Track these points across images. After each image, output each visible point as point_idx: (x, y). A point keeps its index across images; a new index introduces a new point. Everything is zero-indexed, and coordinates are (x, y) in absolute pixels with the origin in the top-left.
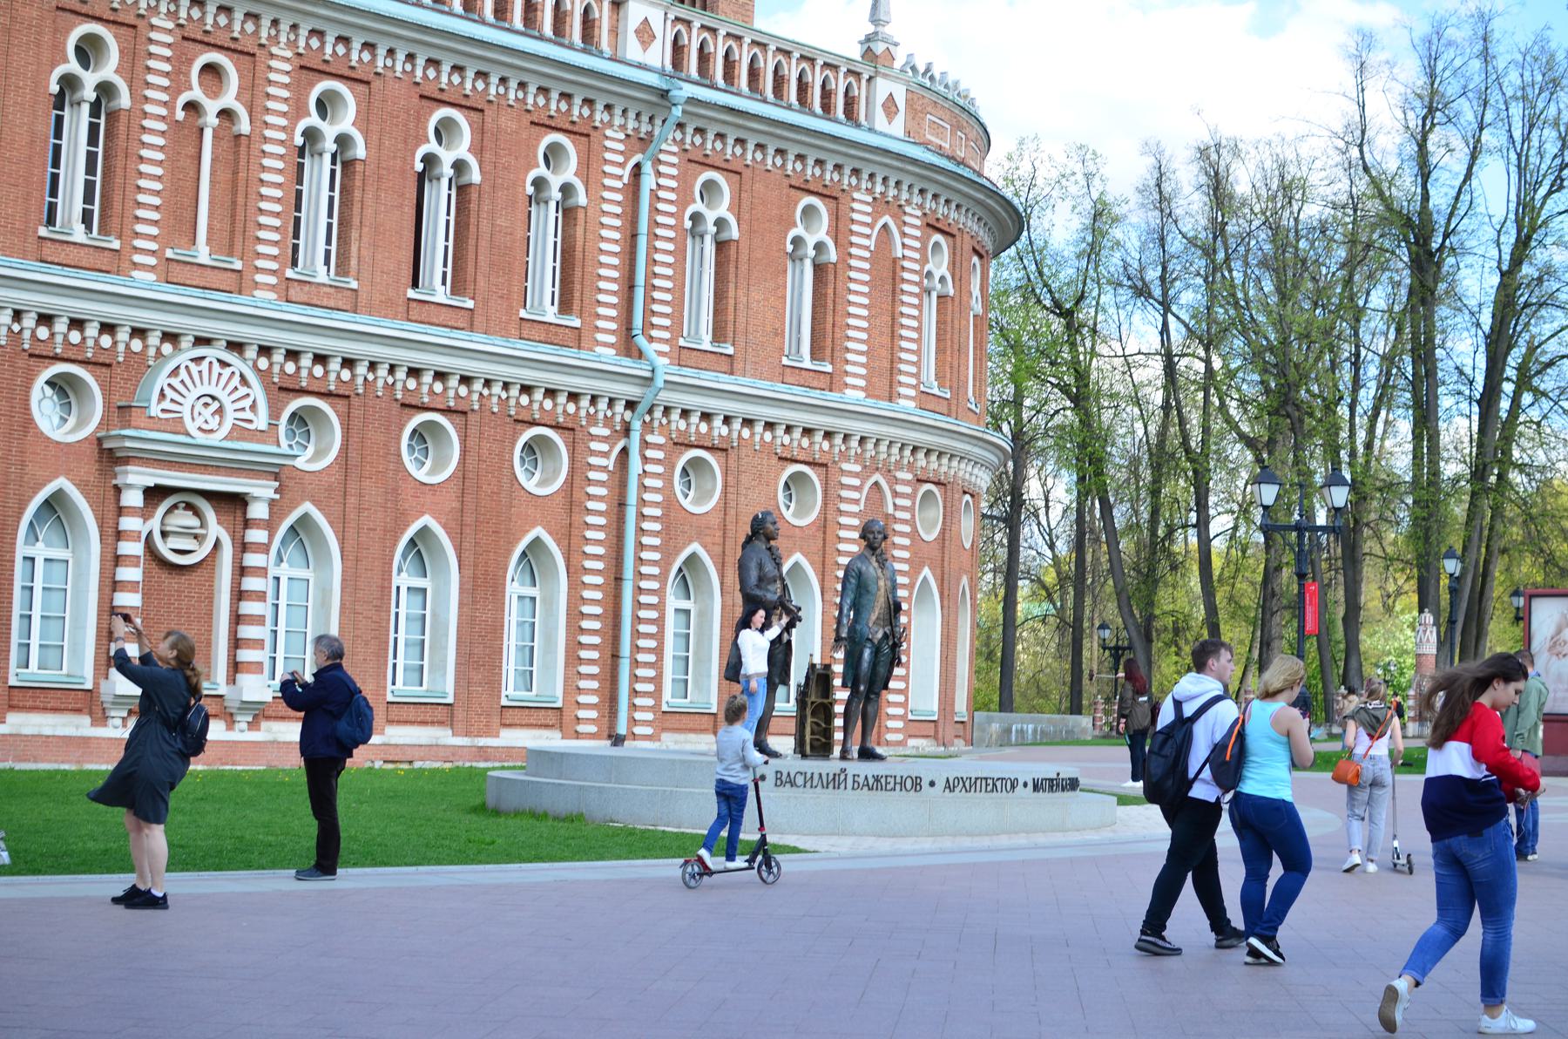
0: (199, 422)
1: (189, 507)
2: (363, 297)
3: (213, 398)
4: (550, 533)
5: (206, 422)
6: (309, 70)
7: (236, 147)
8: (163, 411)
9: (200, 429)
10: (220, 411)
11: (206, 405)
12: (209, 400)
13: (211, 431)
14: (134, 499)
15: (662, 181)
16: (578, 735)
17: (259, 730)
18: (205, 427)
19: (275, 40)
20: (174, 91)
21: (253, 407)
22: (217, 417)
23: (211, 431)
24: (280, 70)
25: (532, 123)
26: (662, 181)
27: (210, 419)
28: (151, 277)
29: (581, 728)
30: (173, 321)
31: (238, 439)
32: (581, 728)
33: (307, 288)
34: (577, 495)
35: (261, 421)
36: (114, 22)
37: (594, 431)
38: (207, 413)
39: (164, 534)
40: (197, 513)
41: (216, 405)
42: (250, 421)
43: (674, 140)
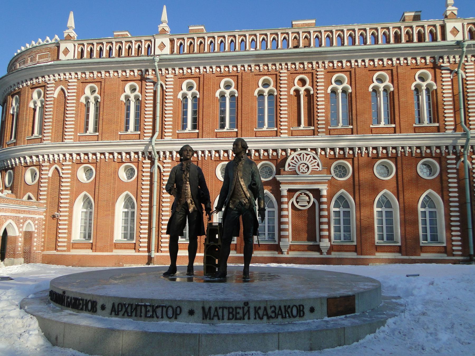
0: (301, 171)
1: (305, 194)
2: (355, 130)
3: (306, 164)
4: (435, 191)
5: (304, 170)
6: (333, 71)
7: (310, 98)
8: (290, 169)
9: (302, 173)
10: (308, 167)
11: (304, 166)
12: (304, 165)
13: (306, 173)
14: (285, 193)
15: (467, 75)
16: (454, 255)
17: (331, 254)
18: (304, 172)
19: (319, 67)
20: (289, 88)
21: (318, 165)
22: (307, 169)
23: (306, 173)
24: (321, 74)
25: (411, 69)
26: (467, 75)
27: (305, 170)
28: (286, 135)
29: (455, 253)
30: (293, 145)
31: (314, 174)
32: (455, 253)
33: (336, 130)
34: (444, 178)
35: (320, 169)
36: (271, 74)
37: (448, 157)
38: (304, 168)
39: (297, 202)
40: (307, 195)
41: (306, 166)
42: (318, 169)
43: (471, 61)
